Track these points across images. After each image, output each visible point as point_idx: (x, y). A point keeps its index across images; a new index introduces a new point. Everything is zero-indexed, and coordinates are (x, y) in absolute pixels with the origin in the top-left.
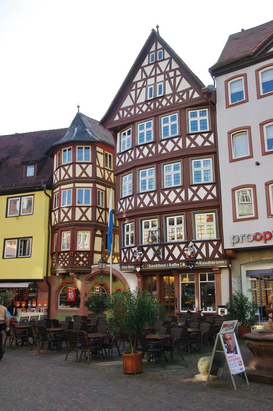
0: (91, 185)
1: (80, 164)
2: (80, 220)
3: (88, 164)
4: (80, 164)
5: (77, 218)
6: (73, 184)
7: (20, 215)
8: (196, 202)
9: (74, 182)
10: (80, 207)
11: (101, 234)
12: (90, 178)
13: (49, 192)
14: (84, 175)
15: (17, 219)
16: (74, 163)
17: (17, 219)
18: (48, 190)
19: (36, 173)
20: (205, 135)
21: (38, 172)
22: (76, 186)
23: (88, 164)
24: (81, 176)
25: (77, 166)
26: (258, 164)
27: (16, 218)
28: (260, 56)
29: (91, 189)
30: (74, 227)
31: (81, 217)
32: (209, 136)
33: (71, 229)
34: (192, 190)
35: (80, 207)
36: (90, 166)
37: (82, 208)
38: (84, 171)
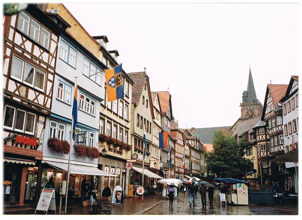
0: (265, 143)
2: (263, 157)
3: (263, 134)
4: (261, 135)
5: (262, 156)
10: (262, 152)
13: (256, 145)
14: (262, 139)
16: (259, 135)
23: (263, 134)
25: (260, 136)
26: (288, 138)
31: (263, 156)
32: (282, 126)
35: (262, 152)
36: (264, 135)
38: (262, 137)
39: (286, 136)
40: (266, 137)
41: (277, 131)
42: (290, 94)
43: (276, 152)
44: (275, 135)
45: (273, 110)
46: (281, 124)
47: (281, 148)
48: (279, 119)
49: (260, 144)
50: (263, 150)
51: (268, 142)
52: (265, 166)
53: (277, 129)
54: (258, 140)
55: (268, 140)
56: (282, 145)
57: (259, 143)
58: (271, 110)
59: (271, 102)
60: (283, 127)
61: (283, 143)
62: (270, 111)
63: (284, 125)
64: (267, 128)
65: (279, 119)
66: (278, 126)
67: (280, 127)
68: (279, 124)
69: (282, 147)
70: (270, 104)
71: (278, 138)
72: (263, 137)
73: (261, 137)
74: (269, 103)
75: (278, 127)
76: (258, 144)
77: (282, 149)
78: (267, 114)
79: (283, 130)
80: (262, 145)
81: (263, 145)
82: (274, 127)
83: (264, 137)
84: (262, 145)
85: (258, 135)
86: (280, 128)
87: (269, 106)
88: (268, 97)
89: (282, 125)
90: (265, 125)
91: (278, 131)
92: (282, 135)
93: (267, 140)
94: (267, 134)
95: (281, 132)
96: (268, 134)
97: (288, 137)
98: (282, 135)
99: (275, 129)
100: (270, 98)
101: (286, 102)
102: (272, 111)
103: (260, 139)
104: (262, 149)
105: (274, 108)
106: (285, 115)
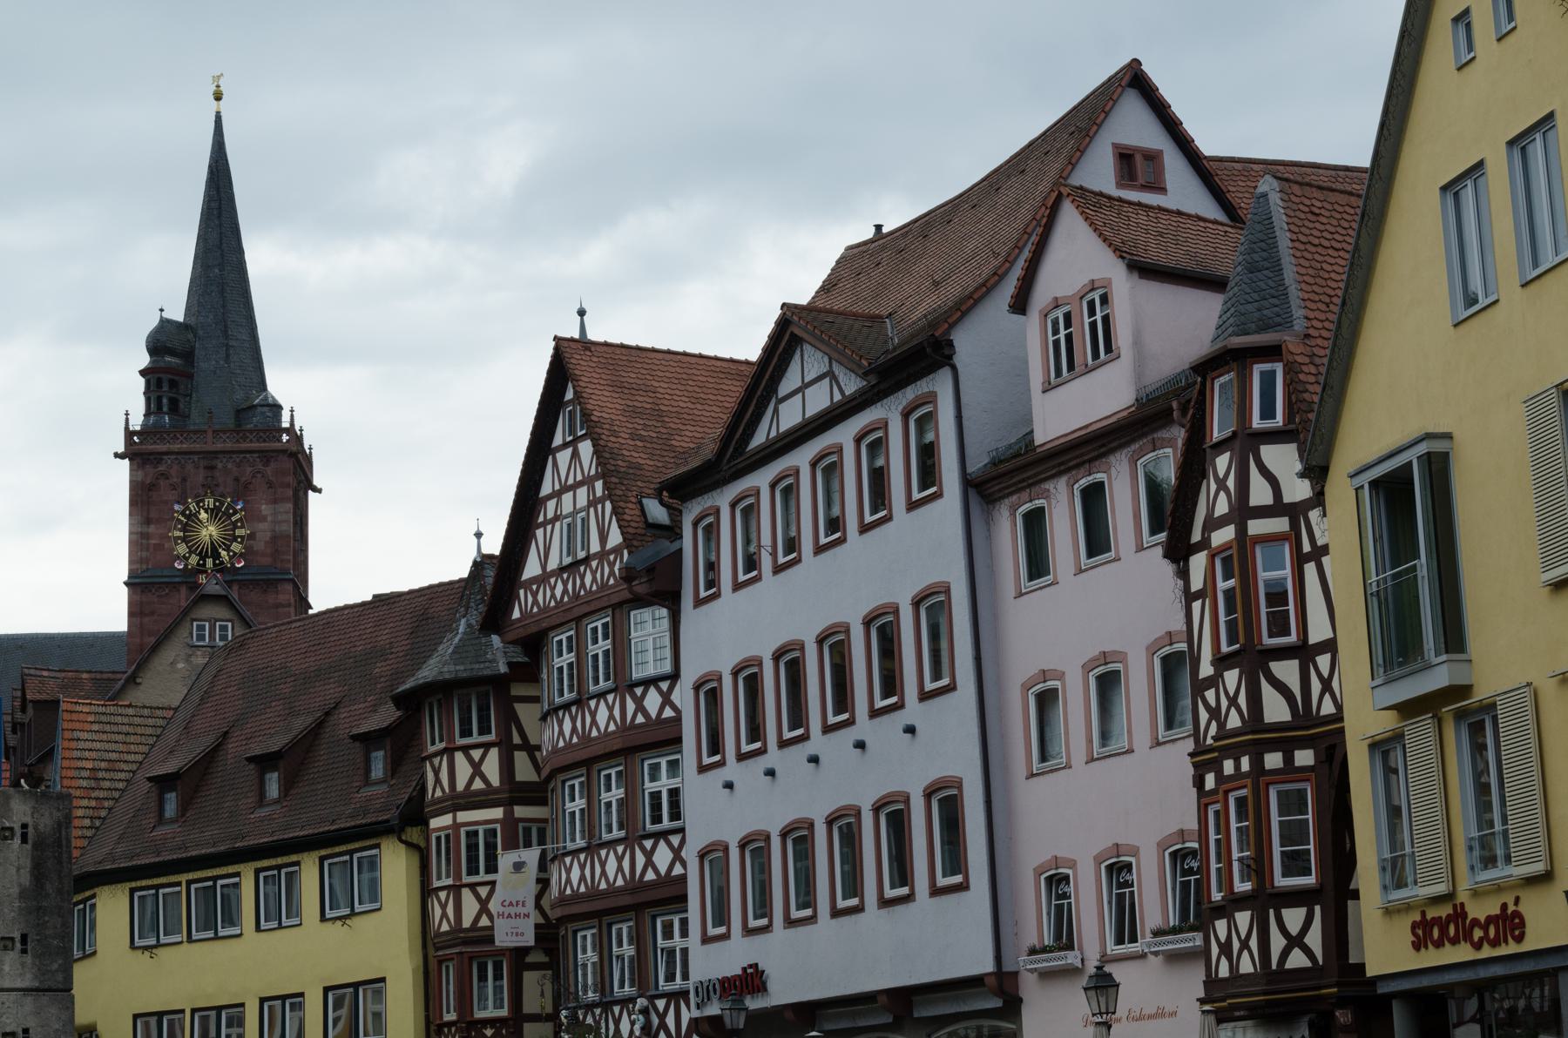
0: (498, 813)
1: (465, 749)
3: (487, 746)
5: (466, 923)
6: (451, 815)
7: (353, 914)
8: (652, 884)
9: (455, 809)
10: (472, 887)
11: (546, 959)
12: (496, 791)
13: (413, 834)
14: (478, 784)
15: (343, 925)
16: (449, 751)
17: (343, 925)
18: (414, 829)
19: (389, 767)
20: (664, 686)
21: (394, 766)
22: (459, 820)
24: (470, 787)
25: (459, 757)
27: (339, 923)
28: (732, 464)
29: (498, 826)
30: (460, 947)
31: (477, 918)
32: (671, 689)
33: (455, 956)
34: (643, 849)
35: (472, 887)
37: (479, 889)
38: (477, 767)
39: (703, 769)
40: (507, 767)
41: (626, 728)
42: (759, 439)
43: (612, 891)
44: (609, 756)
45: (595, 547)
46: (667, 667)
47: (656, 858)
48: (649, 628)
49: (456, 826)
50: (482, 876)
51: (520, 811)
52: (490, 1003)
53: (631, 706)
54: (433, 792)
55: (536, 793)
56: (664, 835)
57: (444, 821)
58: (581, 555)
59: (588, 481)
60: (683, 695)
61: (666, 823)
62: (567, 561)
63: (689, 676)
64: (517, 690)
65: (648, 626)
66: (638, 684)
67: (652, 691)
68: (650, 671)
69: (663, 856)
70: (567, 498)
71: (630, 782)
72: (484, 768)
73: (463, 770)
74: (565, 489)
75: (639, 691)
76: (435, 823)
77: (663, 871)
78: (543, 579)
79: (678, 720)
80: (472, 835)
81: (481, 829)
82: (601, 695)
83: (492, 767)
84: (472, 835)
85: (440, 753)
86: (653, 701)
87: (556, 518)
88: (558, 440)
89: (674, 677)
90: (503, 668)
91: (633, 726)
92: (663, 762)
93: (513, 793)
94: (517, 740)
95: (665, 737)
96: (531, 749)
97: (727, 773)
98: (663, 762)
99: (610, 709)
100: (575, 455)
101: (723, 499)
102: (586, 561)
103: (460, 786)
104: (473, 870)
105: (615, 538)
106: (699, 602)
